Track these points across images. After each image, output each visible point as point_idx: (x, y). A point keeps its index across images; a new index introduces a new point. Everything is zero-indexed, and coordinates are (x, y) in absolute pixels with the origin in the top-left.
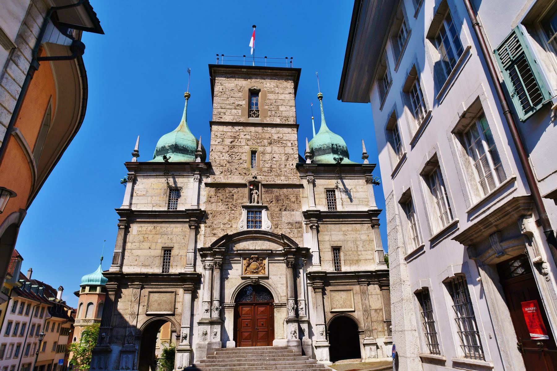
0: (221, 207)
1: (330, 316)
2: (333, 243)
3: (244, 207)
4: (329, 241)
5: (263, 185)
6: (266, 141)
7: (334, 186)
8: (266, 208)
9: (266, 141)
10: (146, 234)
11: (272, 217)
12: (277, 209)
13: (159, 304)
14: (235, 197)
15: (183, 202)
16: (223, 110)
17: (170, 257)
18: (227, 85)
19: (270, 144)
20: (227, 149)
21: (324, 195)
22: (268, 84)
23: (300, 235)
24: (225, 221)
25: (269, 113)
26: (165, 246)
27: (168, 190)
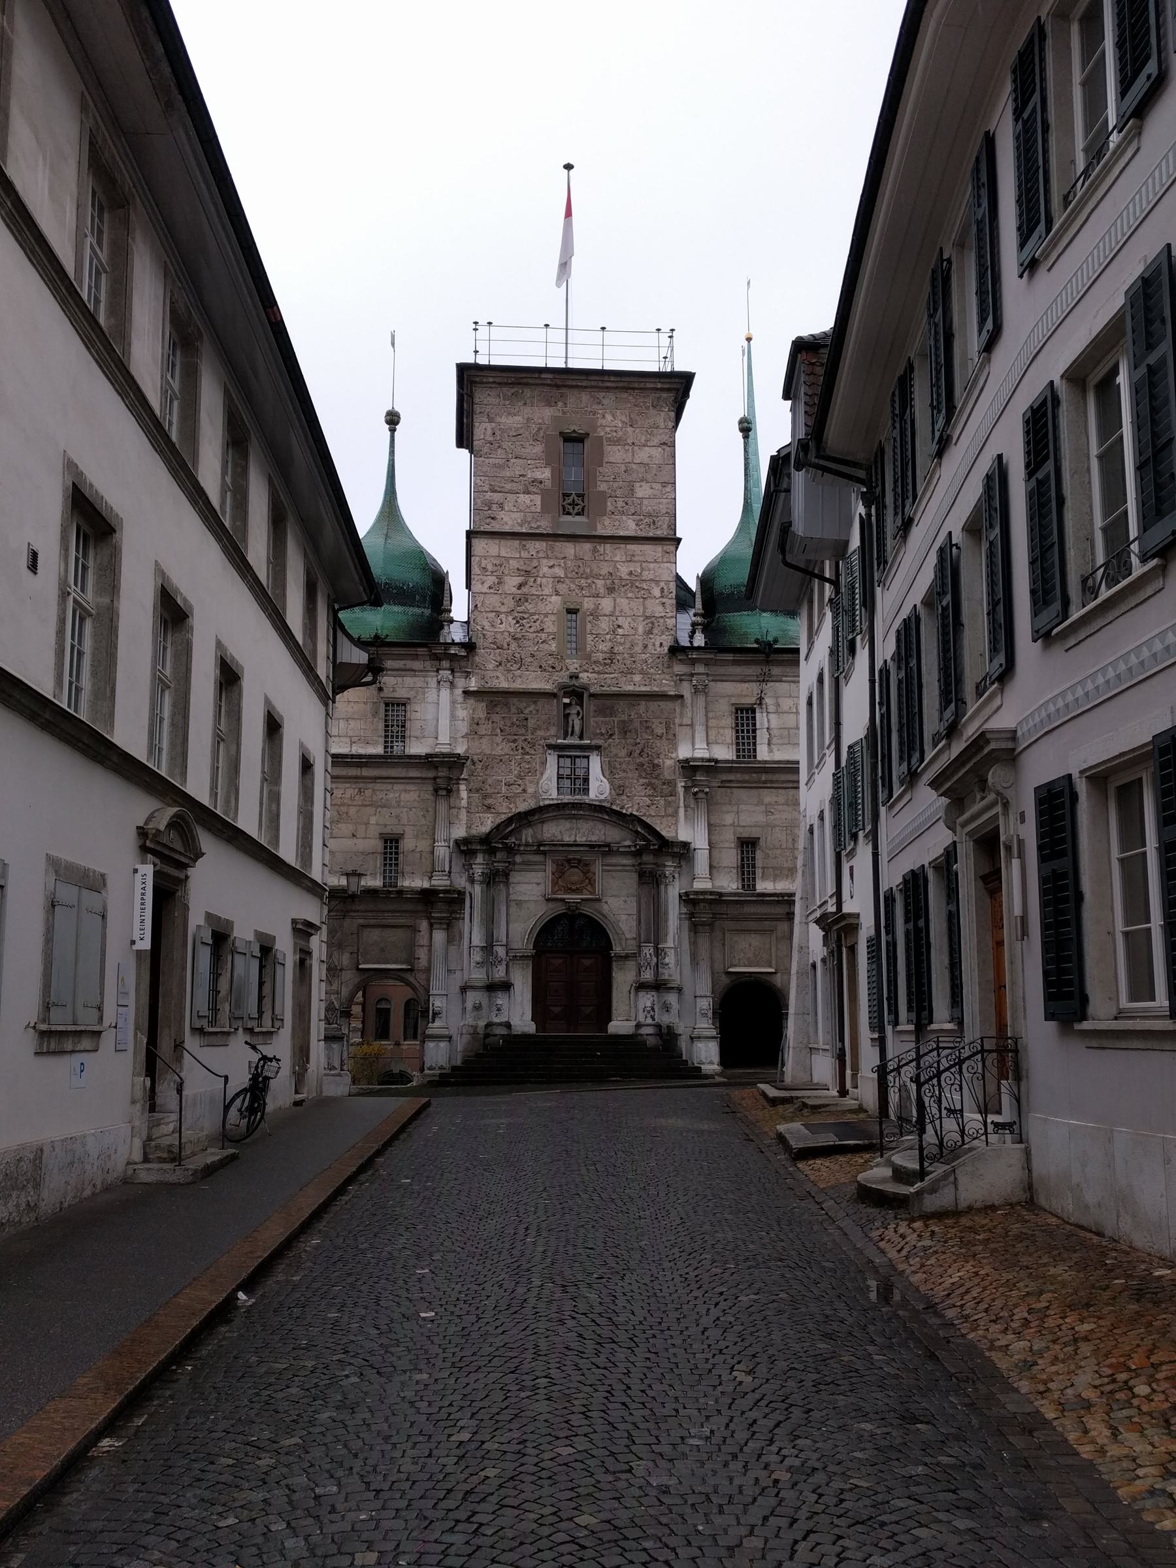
0: (502, 748)
1: (725, 980)
2: (741, 830)
3: (550, 747)
4: (733, 825)
5: (592, 695)
6: (600, 583)
7: (752, 700)
8: (598, 748)
9: (600, 583)
10: (343, 805)
11: (610, 770)
12: (623, 753)
13: (382, 950)
14: (531, 723)
15: (418, 733)
16: (497, 497)
17: (397, 853)
18: (503, 420)
19: (611, 590)
20: (511, 603)
21: (729, 721)
22: (609, 417)
23: (670, 810)
24: (511, 778)
25: (610, 507)
26: (386, 831)
27: (383, 706)
